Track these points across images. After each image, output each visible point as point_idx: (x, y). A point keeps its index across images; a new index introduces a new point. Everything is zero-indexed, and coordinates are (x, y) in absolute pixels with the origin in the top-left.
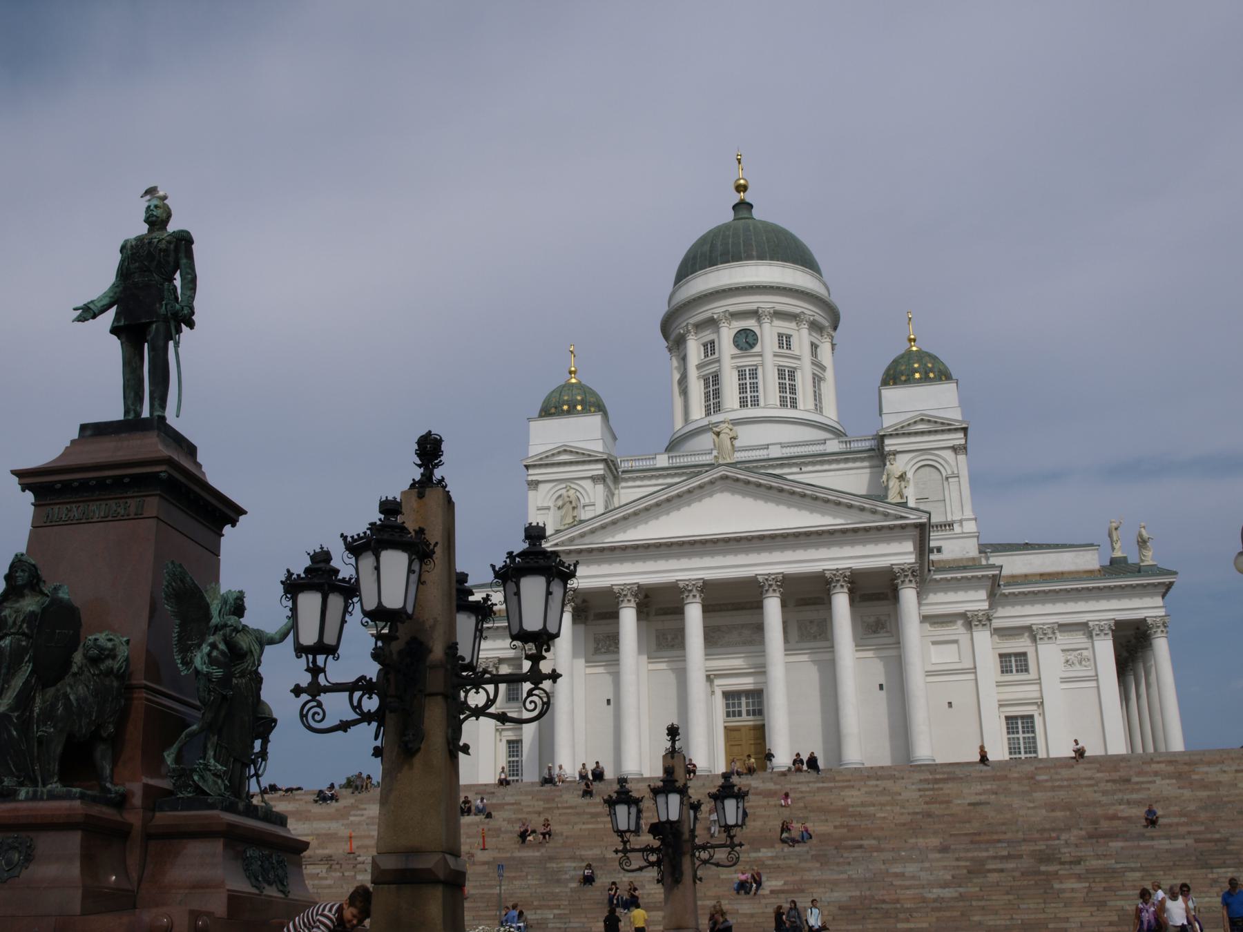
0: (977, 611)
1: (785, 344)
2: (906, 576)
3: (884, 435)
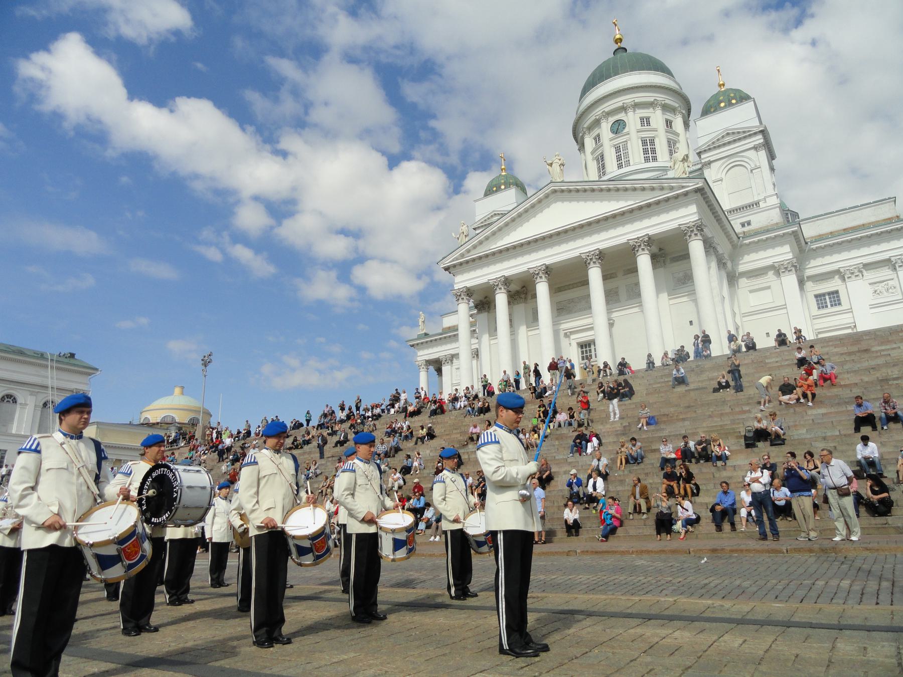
0: (783, 261)
1: (645, 122)
2: (692, 231)
3: (700, 152)
